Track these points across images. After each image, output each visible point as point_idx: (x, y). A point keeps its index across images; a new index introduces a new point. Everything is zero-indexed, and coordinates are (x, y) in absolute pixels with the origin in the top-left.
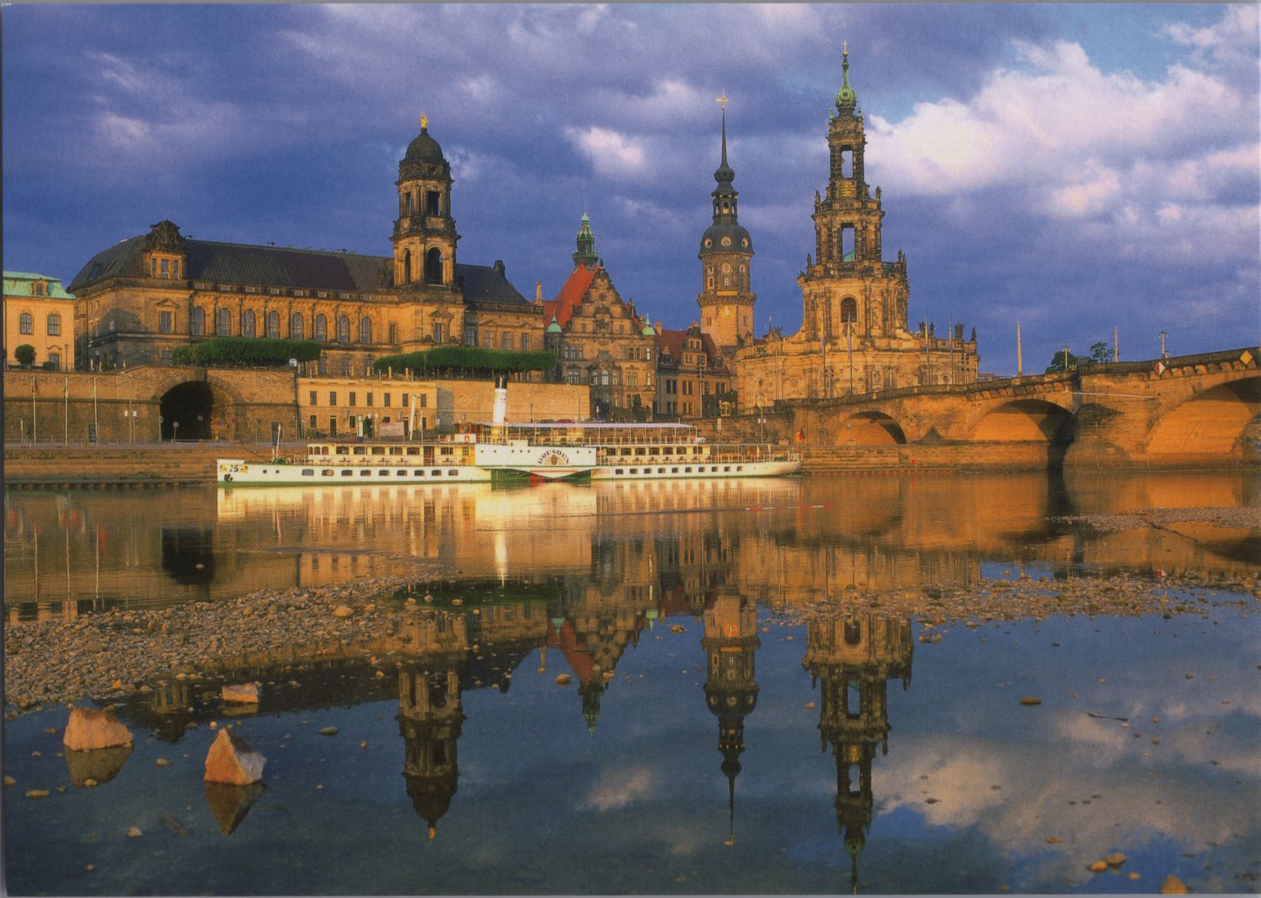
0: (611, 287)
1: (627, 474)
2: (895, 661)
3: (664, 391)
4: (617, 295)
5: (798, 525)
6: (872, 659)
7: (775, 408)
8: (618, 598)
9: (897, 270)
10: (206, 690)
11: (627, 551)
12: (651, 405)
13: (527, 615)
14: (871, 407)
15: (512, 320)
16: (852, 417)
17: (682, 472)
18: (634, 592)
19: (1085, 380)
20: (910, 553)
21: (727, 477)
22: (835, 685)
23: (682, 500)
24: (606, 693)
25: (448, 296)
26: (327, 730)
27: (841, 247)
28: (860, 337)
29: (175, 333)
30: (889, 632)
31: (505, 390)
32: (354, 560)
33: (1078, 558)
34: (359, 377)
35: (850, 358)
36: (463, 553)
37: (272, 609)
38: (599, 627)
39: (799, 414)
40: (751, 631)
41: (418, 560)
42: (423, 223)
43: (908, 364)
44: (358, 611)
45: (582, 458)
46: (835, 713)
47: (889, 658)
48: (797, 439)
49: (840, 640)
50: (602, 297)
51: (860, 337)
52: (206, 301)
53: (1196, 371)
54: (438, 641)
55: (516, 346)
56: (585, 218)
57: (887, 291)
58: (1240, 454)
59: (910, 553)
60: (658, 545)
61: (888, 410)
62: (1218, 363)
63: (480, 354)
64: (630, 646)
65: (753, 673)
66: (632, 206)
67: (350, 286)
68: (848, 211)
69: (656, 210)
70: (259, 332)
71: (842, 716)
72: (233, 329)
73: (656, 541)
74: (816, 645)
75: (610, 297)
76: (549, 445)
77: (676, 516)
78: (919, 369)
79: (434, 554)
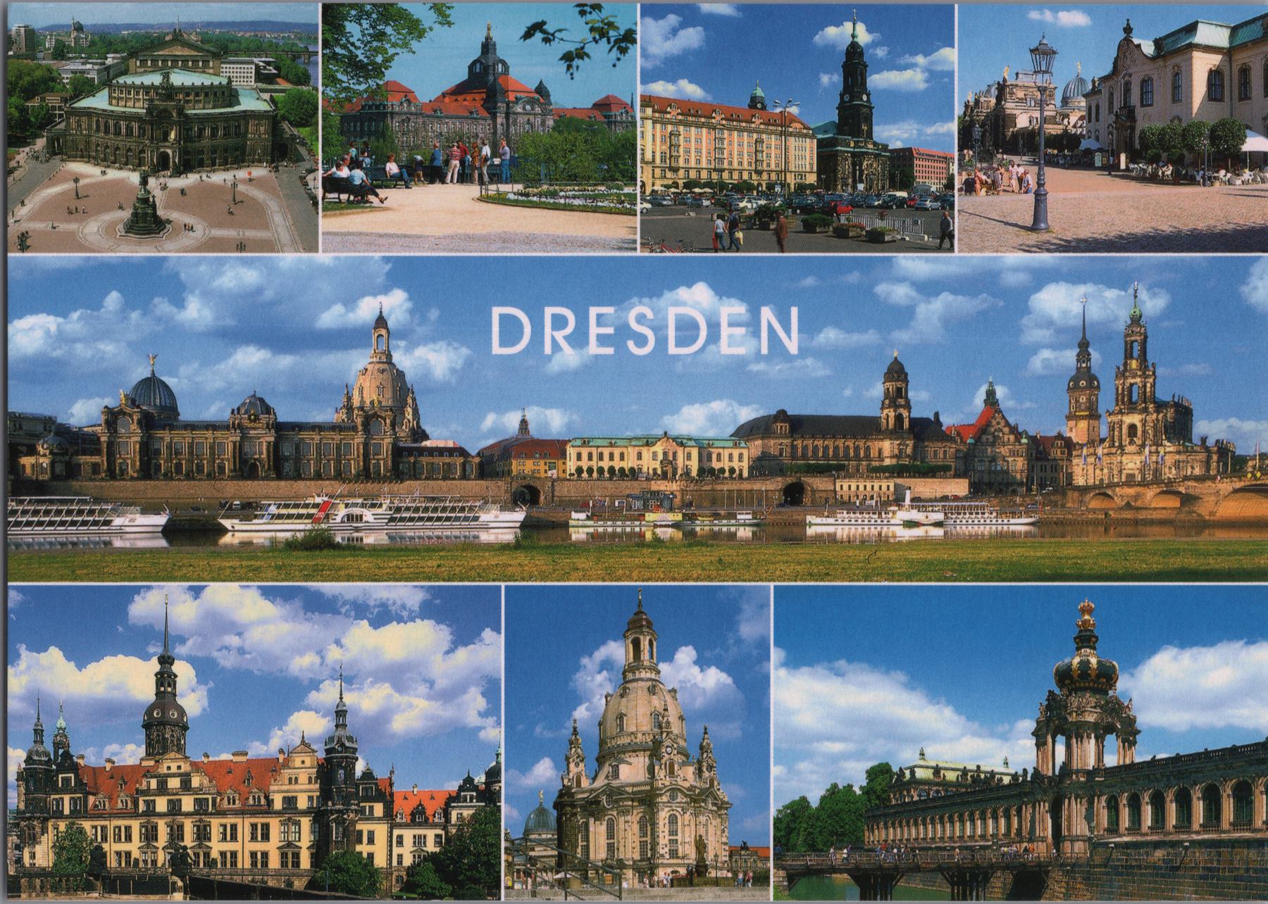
15: (939, 444)
68: (1134, 377)
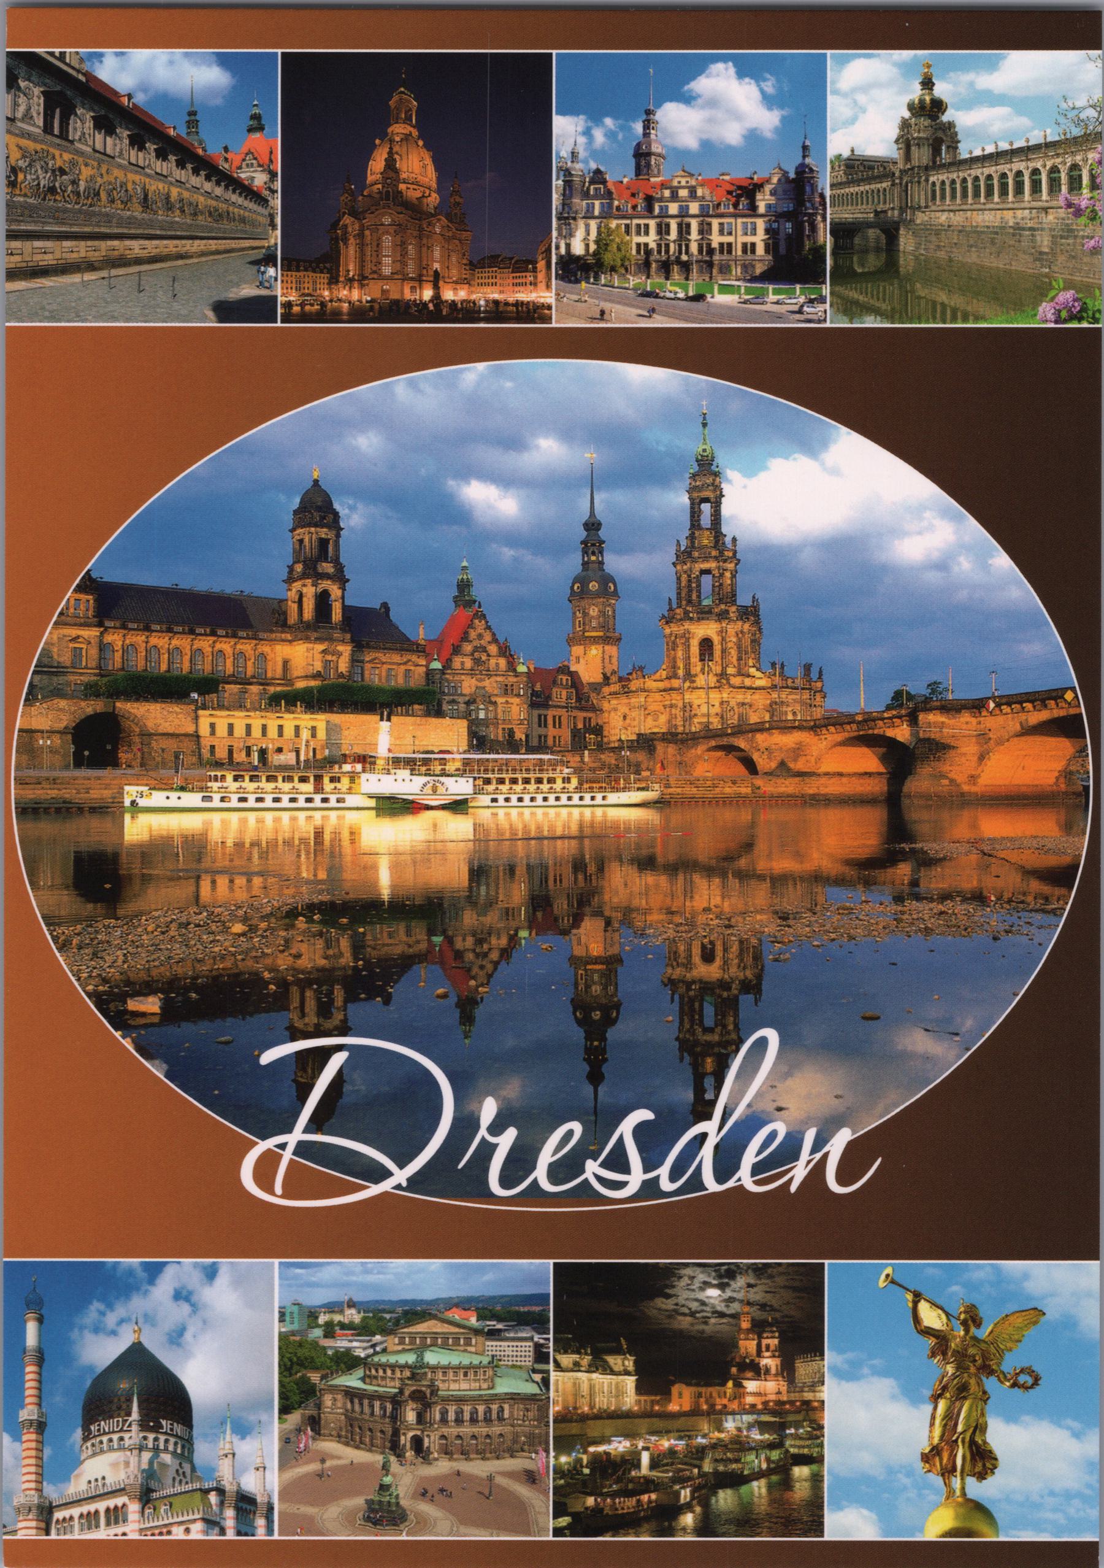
0: (488, 628)
1: (501, 802)
2: (746, 978)
3: (535, 726)
4: (494, 634)
5: (658, 850)
6: (726, 976)
7: (637, 741)
8: (492, 918)
9: (750, 613)
10: (113, 1001)
11: (501, 874)
12: (523, 738)
13: (408, 933)
14: (725, 741)
15: (396, 658)
16: (709, 750)
17: (552, 800)
18: (508, 913)
19: (921, 716)
20: (761, 878)
21: (593, 806)
22: (692, 1001)
23: (552, 828)
24: (481, 1006)
25: (337, 635)
26: (223, 1039)
27: (699, 592)
28: (716, 675)
29: (86, 668)
30: (741, 950)
31: (388, 723)
32: (249, 881)
33: (915, 883)
34: (255, 709)
35: (707, 694)
36: (349, 875)
37: (173, 926)
38: (475, 944)
39: (660, 747)
40: (615, 950)
41: (308, 882)
42: (315, 568)
43: (761, 700)
44: (253, 929)
45: (460, 787)
46: (692, 1026)
47: (741, 976)
48: (658, 770)
49: (697, 959)
50: (480, 637)
51: (716, 675)
52: (115, 638)
53: (1023, 708)
54: (326, 958)
55: (400, 682)
56: (465, 564)
57: (742, 632)
58: (1063, 786)
59: (761, 878)
60: (529, 867)
61: (741, 743)
62: (1043, 701)
63: (368, 689)
64: (503, 962)
65: (616, 989)
66: (508, 553)
67: (247, 625)
68: (706, 559)
69: (530, 557)
70: (164, 667)
71: (699, 1030)
72: (139, 663)
73: (528, 865)
74: (675, 964)
75: (488, 637)
76: (430, 775)
77: (546, 842)
78: (771, 705)
79: (322, 875)
